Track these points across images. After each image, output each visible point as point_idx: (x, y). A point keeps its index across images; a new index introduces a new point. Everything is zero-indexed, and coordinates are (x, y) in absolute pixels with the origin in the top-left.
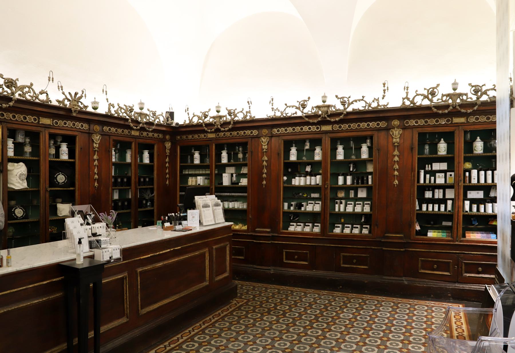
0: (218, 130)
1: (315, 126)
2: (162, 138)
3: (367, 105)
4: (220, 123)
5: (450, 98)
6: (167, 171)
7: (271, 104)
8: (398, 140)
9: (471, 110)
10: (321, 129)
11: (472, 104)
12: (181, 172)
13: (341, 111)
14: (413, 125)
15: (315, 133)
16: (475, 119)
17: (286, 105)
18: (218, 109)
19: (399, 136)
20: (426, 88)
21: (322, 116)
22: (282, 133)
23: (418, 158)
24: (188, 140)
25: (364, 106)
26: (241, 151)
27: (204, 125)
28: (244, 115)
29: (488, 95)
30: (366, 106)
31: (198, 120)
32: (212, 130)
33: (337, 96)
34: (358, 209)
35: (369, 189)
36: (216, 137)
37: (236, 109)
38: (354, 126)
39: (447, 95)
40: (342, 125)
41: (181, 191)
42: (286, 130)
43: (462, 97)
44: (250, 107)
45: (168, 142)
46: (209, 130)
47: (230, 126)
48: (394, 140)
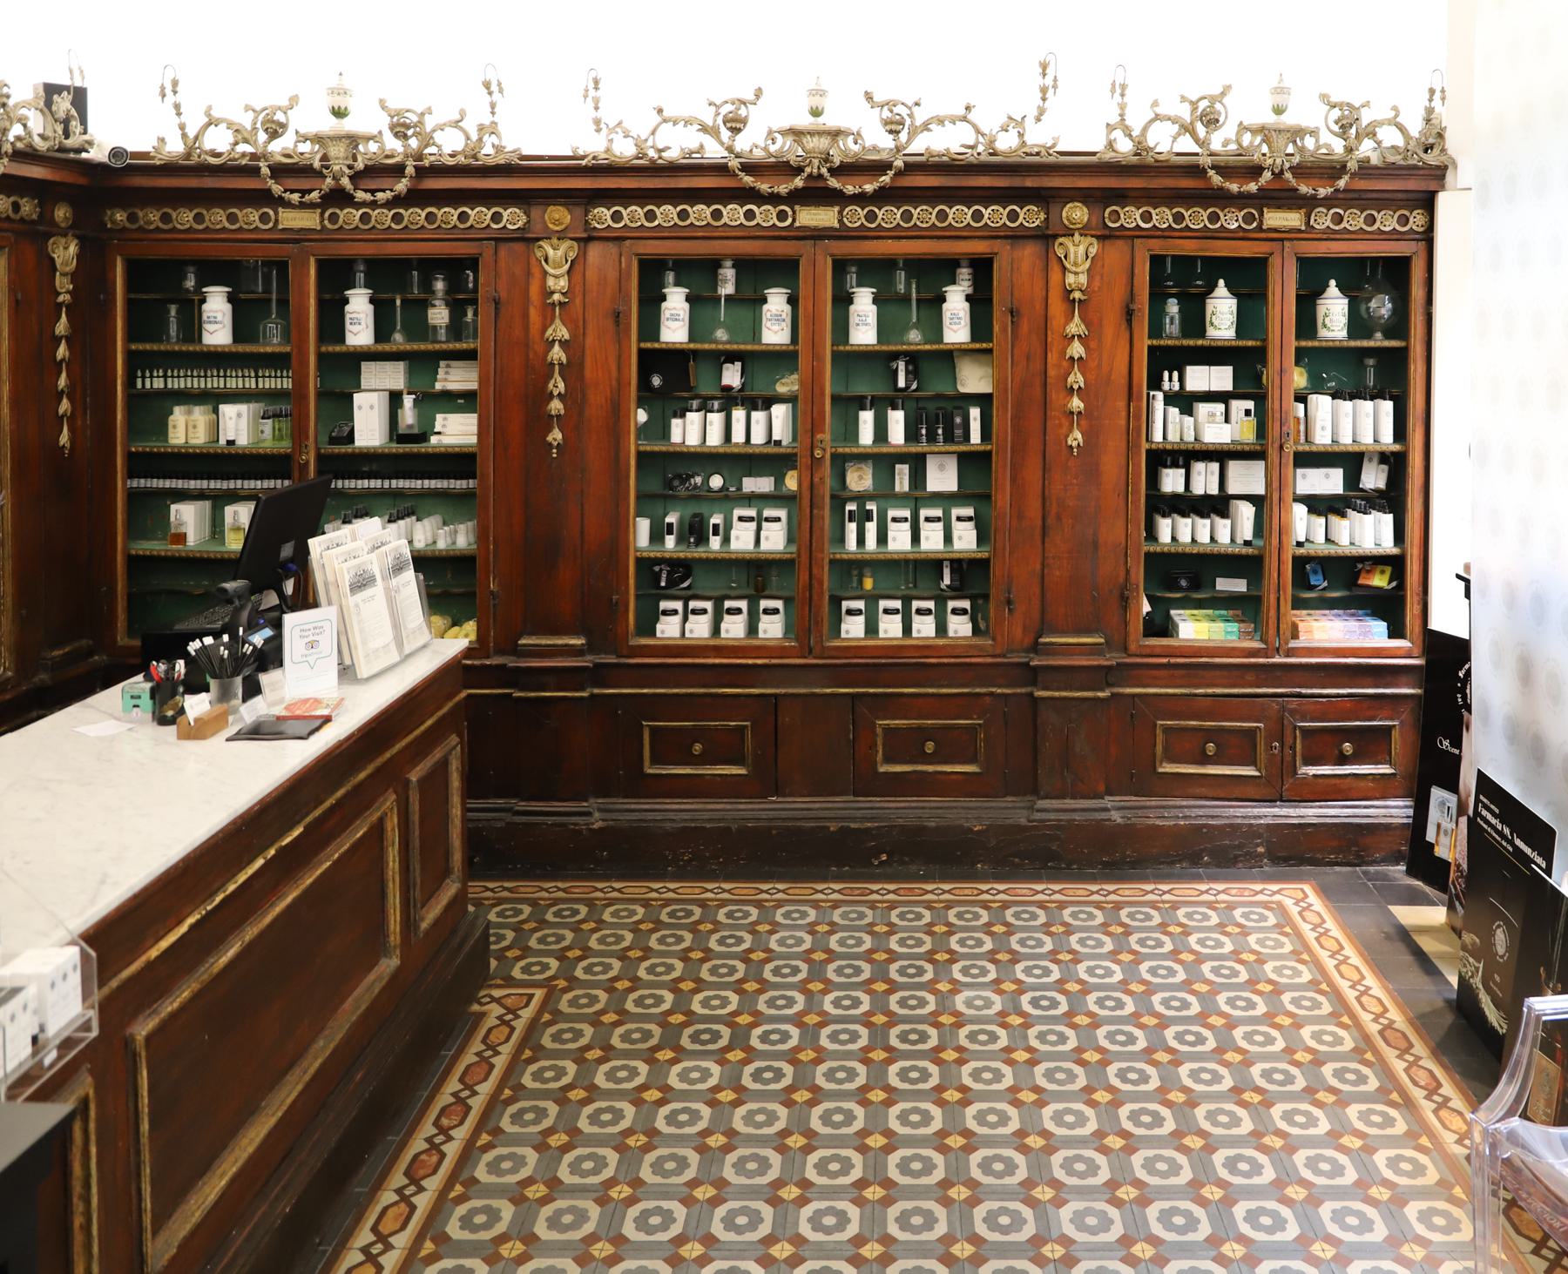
0: (338, 197)
1: (769, 207)
2: (35, 217)
3: (981, 139)
4: (350, 167)
5: (1263, 141)
6: (62, 381)
7: (589, 99)
8: (1083, 279)
9: (1330, 190)
10: (794, 220)
11: (1333, 170)
12: (130, 382)
13: (884, 156)
15: (774, 235)
16: (1332, 220)
17: (660, 111)
18: (339, 102)
20: (1186, 95)
21: (808, 170)
22: (633, 225)
23: (1151, 348)
24: (174, 230)
26: (440, 295)
27: (265, 171)
28: (468, 138)
29: (1379, 143)
31: (236, 143)
32: (307, 197)
33: (869, 97)
34: (932, 539)
35: (973, 464)
36: (323, 227)
37: (429, 111)
38: (924, 215)
39: (1255, 131)
40: (876, 210)
41: (131, 474)
42: (650, 216)
43: (1302, 139)
44: (493, 106)
45: (63, 240)
46: (295, 197)
47: (402, 186)
48: (1070, 279)
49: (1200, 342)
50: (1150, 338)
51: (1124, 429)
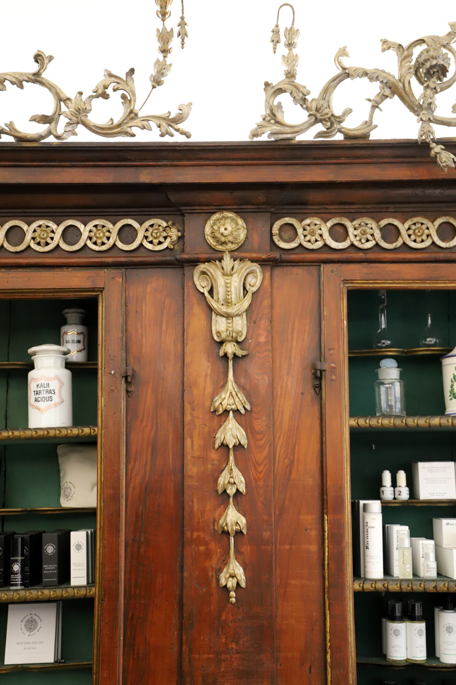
14: (320, 244)
19: (246, 303)
20: (391, 39)
25: (49, 112)
30: (58, 113)
49: (436, 421)
50: (352, 415)
51: (315, 558)
